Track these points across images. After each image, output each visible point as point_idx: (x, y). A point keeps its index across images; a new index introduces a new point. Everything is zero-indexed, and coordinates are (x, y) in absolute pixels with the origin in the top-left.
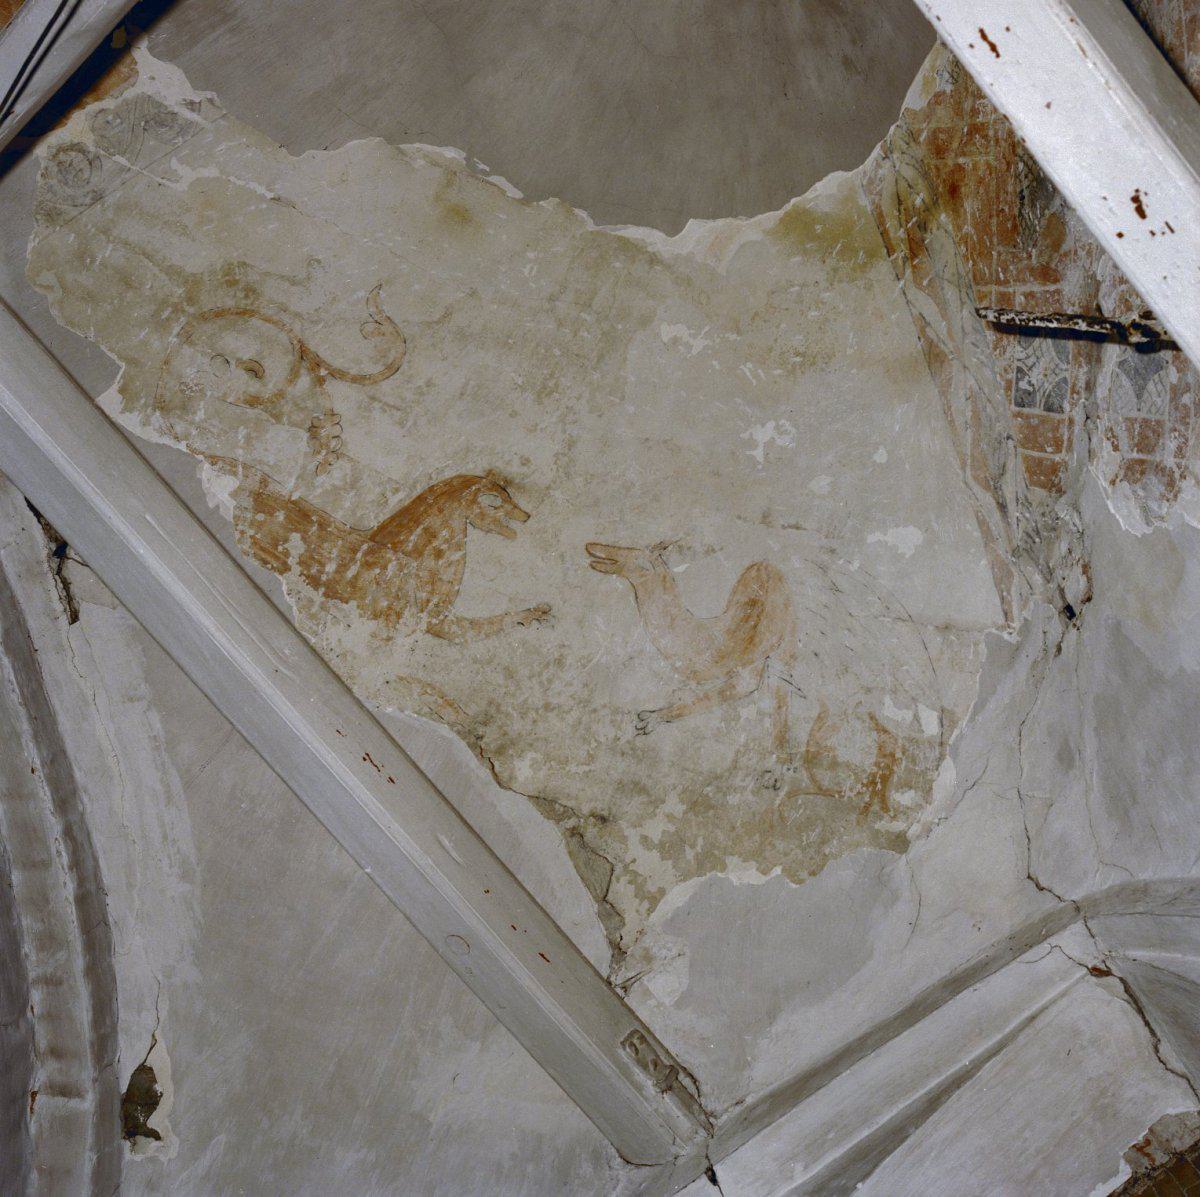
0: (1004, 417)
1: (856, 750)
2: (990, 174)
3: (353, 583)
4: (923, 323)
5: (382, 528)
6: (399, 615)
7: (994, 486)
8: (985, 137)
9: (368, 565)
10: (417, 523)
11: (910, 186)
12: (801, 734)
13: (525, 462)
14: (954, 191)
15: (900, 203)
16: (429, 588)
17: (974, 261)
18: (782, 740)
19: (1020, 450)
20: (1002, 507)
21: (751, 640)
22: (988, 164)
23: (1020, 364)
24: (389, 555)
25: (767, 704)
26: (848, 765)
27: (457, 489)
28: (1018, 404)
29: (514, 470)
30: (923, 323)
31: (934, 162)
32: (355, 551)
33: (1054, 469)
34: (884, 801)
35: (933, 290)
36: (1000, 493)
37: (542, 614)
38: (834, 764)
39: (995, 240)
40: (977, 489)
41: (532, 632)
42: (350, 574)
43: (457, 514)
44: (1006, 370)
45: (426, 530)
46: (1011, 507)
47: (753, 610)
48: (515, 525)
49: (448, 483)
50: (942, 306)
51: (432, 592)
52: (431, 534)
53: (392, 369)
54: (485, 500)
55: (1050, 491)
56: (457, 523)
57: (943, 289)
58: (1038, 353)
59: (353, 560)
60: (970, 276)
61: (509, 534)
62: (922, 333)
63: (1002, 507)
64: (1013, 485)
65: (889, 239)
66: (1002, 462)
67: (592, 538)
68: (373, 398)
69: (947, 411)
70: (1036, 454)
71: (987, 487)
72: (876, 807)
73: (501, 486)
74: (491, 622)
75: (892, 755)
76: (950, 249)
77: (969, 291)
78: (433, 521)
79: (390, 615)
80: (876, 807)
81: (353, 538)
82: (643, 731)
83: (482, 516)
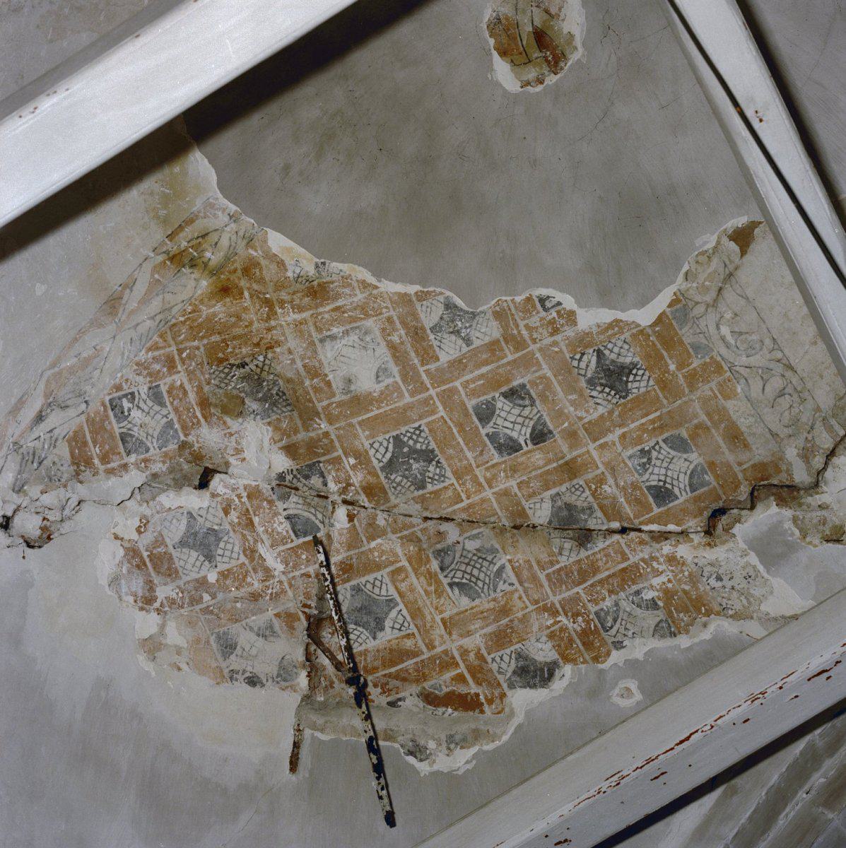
0: (99, 390)
2: (246, 326)
7: (54, 403)
8: (269, 318)
11: (216, 244)
15: (203, 236)
17: (185, 321)
19: (83, 418)
20: (40, 418)
22: (251, 323)
23: (136, 394)
28: (111, 401)
30: (129, 285)
31: (239, 267)
33: (89, 462)
35: (155, 286)
36: (49, 411)
39: (205, 341)
40: (42, 386)
44: (127, 380)
50: (145, 301)
55: (73, 463)
57: (157, 295)
58: (152, 413)
60: (174, 321)
63: (40, 418)
64: (63, 422)
65: (178, 234)
66: (69, 403)
69: (82, 332)
71: (47, 396)
76: (185, 295)
77: (163, 322)
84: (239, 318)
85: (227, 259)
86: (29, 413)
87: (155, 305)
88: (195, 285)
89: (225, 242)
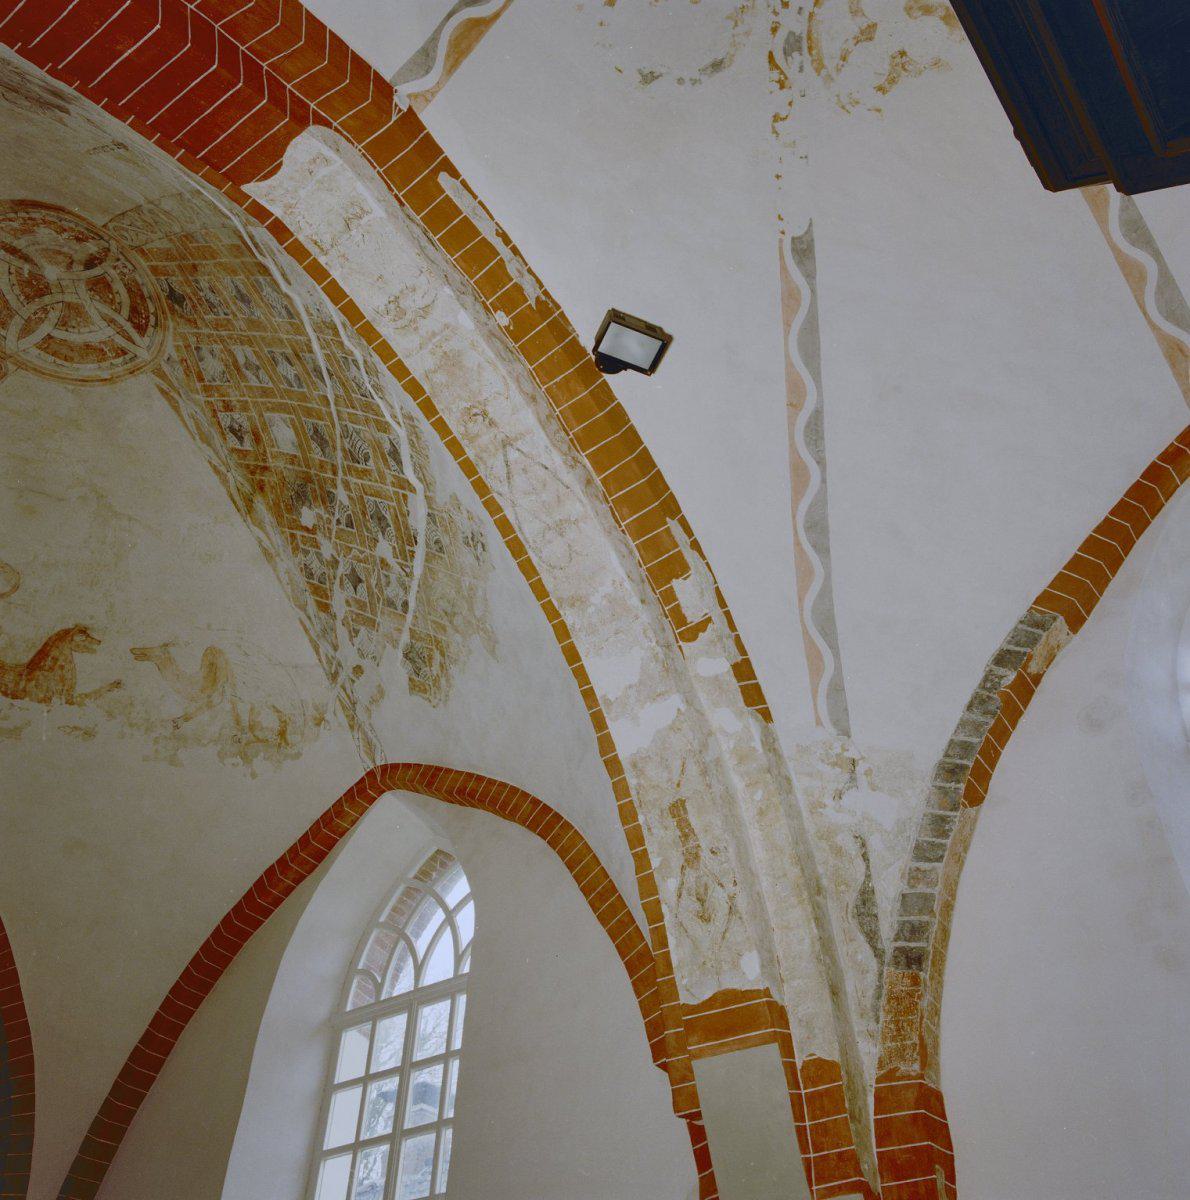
0: (301, 580)
1: (270, 722)
3: (24, 690)
4: (260, 542)
5: (32, 661)
6: (50, 699)
9: (29, 680)
10: (47, 656)
12: (245, 718)
13: (92, 618)
14: (262, 489)
15: (238, 490)
16: (61, 684)
18: (238, 722)
20: (309, 618)
21: (215, 680)
24: (38, 673)
25: (228, 707)
26: (267, 728)
27: (64, 635)
29: (87, 622)
30: (260, 542)
32: (21, 675)
34: (286, 741)
35: (260, 525)
37: (118, 684)
38: (262, 729)
41: (116, 693)
42: (21, 687)
43: (66, 647)
45: (53, 658)
46: (313, 618)
47: (213, 667)
48: (95, 647)
49: (58, 634)
50: (267, 534)
51: (64, 685)
52: (55, 659)
53: (16, 587)
54: (78, 638)
56: (67, 651)
59: (21, 680)
61: (94, 651)
62: (261, 545)
63: (309, 618)
64: (312, 608)
67: (132, 647)
68: (10, 603)
70: (318, 599)
72: (283, 744)
73: (83, 631)
74: (95, 693)
75: (285, 722)
78: (55, 653)
79: (47, 700)
80: (283, 744)
81: (19, 669)
82: (177, 727)
83: (78, 646)
84: (273, 487)
85: (248, 481)
86: (307, 623)
87: (269, 528)
88: (260, 505)
89: (239, 478)
